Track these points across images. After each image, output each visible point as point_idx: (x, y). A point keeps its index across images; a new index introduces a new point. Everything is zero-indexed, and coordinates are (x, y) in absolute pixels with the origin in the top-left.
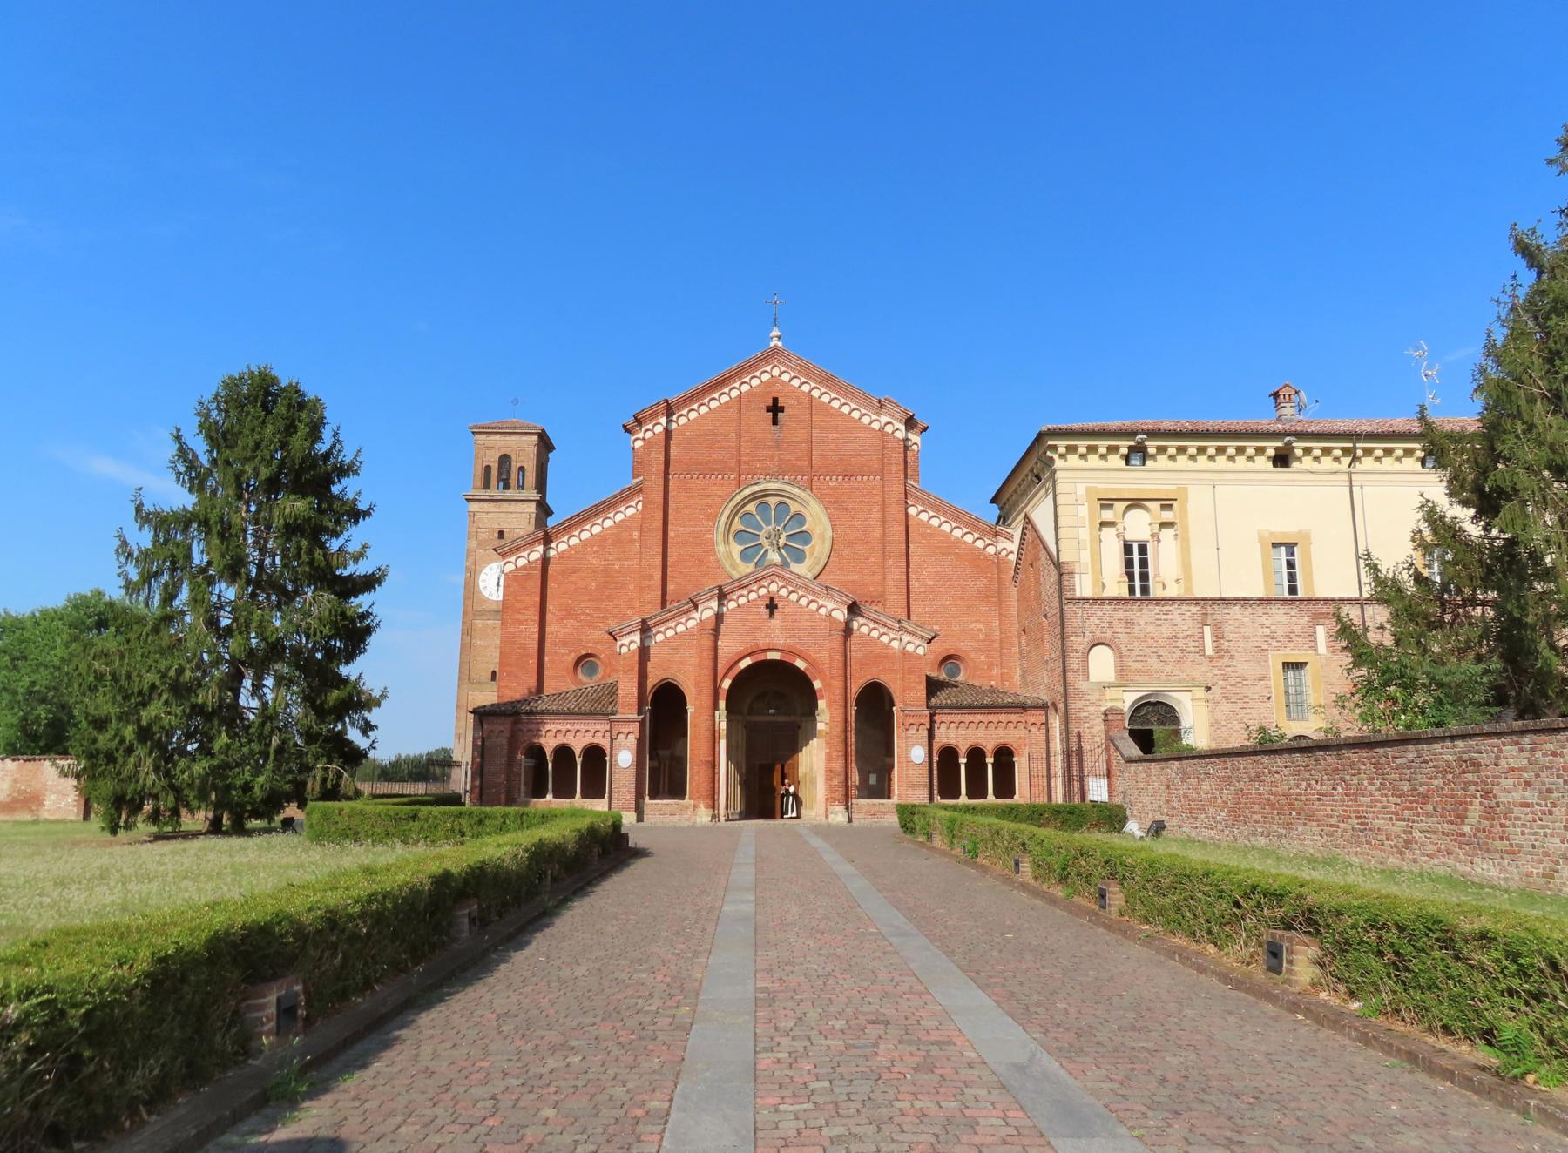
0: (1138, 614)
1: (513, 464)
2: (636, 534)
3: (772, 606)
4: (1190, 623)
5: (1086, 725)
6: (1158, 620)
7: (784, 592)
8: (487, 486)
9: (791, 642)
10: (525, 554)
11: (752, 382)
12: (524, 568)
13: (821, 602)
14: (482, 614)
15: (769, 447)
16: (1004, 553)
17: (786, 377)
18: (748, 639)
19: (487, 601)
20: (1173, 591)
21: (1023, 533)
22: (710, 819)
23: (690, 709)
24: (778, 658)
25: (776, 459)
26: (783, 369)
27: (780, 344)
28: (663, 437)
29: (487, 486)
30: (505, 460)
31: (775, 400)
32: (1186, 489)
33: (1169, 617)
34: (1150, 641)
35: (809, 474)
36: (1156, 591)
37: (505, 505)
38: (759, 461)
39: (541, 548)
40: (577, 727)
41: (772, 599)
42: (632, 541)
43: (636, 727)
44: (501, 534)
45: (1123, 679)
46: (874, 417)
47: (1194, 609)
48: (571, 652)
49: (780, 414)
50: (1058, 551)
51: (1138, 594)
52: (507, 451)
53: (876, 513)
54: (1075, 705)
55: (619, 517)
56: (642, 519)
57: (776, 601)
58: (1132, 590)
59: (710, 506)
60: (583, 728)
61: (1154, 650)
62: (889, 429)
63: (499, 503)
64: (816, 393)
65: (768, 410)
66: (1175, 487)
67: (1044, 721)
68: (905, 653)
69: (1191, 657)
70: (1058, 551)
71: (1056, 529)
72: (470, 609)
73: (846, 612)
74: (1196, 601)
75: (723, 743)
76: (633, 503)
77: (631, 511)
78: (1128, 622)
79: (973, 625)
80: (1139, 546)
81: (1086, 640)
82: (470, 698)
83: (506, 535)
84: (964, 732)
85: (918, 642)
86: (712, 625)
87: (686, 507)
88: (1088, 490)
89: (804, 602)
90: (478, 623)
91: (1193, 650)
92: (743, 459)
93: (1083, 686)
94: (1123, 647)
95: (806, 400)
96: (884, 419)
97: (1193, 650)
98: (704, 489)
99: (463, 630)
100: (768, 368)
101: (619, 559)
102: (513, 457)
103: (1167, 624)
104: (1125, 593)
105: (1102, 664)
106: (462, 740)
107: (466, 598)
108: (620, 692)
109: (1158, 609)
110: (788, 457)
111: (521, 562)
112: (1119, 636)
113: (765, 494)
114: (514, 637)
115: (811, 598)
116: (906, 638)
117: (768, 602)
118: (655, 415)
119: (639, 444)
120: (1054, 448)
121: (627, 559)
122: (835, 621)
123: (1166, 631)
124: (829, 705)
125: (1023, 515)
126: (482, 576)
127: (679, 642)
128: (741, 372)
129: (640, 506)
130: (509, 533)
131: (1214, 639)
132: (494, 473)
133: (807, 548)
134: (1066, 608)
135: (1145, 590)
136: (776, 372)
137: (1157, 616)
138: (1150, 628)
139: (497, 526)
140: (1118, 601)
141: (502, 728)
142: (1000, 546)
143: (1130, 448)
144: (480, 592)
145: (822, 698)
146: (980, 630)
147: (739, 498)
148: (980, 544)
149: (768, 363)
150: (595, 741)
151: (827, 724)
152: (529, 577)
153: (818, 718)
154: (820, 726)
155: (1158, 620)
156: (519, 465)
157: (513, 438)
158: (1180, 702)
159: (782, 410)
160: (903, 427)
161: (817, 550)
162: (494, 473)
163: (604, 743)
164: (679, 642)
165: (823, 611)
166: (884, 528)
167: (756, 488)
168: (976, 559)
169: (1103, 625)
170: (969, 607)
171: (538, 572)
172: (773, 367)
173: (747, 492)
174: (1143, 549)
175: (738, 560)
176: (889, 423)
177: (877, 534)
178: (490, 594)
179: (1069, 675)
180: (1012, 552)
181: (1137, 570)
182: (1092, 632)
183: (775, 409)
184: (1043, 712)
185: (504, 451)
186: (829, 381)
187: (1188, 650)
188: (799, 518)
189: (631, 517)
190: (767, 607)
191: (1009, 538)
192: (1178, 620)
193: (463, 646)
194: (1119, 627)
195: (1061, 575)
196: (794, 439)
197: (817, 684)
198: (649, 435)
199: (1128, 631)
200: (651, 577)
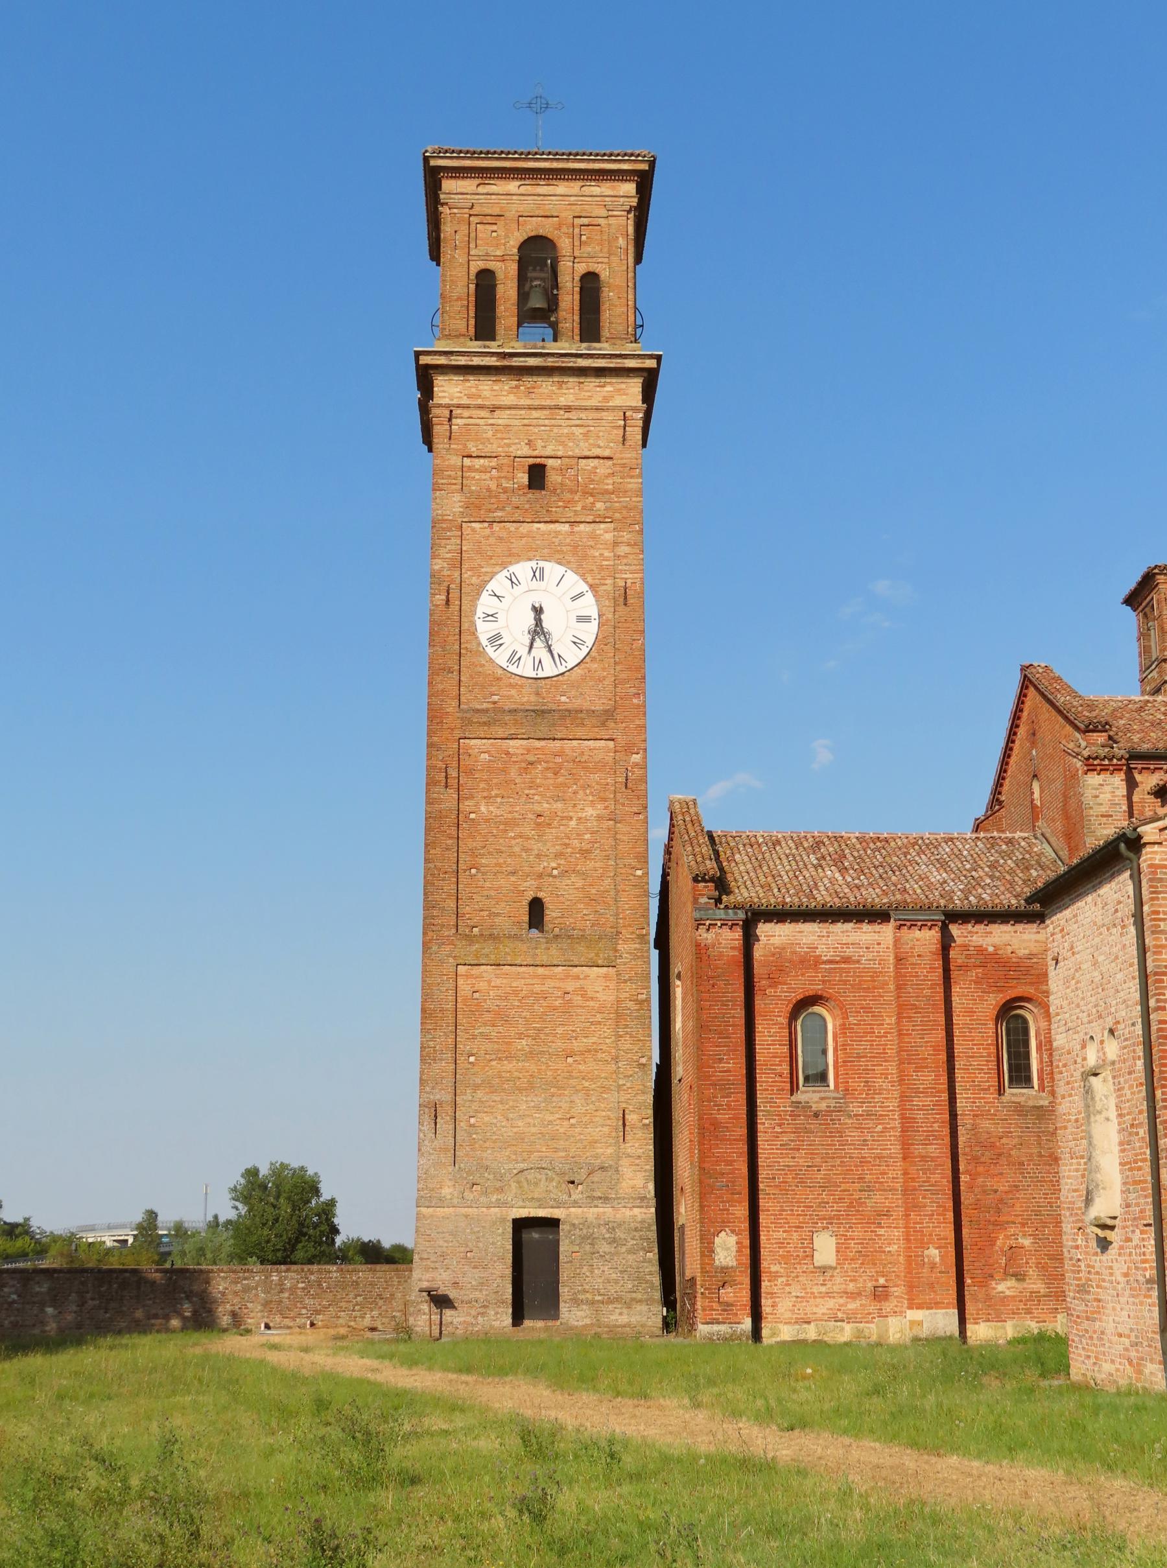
1: (565, 265)
8: (485, 328)
14: (493, 717)
19: (501, 678)
29: (485, 328)
37: (546, 387)
44: (537, 475)
52: (545, 228)
63: (529, 381)
82: (464, 987)
83: (553, 478)
90: (480, 749)
99: (430, 768)
102: (564, 245)
106: (444, 1124)
107: (436, 671)
126: (485, 604)
132: (507, 292)
139: (526, 451)
144: (483, 653)
156: (581, 269)
157: (562, 188)
162: (507, 292)
178: (514, 658)
193: (433, 822)
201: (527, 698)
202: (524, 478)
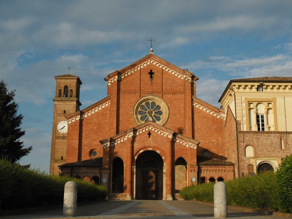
0: (261, 136)
1: (69, 88)
2: (108, 112)
3: (149, 134)
4: (277, 139)
5: (245, 170)
6: (267, 138)
7: (153, 130)
9: (155, 145)
10: (74, 118)
11: (144, 65)
12: (74, 122)
13: (164, 133)
14: (59, 138)
15: (150, 85)
16: (222, 118)
17: (154, 64)
18: (142, 144)
20: (272, 129)
21: (227, 112)
22: (130, 199)
23: (125, 165)
24: (151, 150)
25: (152, 89)
26: (154, 61)
27: (153, 53)
28: (116, 82)
30: (66, 87)
31: (151, 70)
32: (276, 98)
33: (270, 137)
34: (264, 145)
35: (162, 94)
36: (266, 129)
38: (146, 89)
39: (79, 116)
40: (90, 171)
41: (149, 132)
42: (107, 114)
43: (108, 171)
44: (65, 112)
45: (256, 157)
46: (182, 75)
47: (278, 135)
48: (88, 148)
49: (153, 75)
50: (236, 117)
51: (261, 130)
53: (182, 105)
54: (241, 164)
55: (103, 107)
56: (110, 107)
57: (151, 132)
58: (259, 129)
59: (131, 103)
60: (92, 171)
61: (265, 147)
62: (186, 79)
64: (164, 68)
65: (149, 73)
66: (272, 98)
67: (233, 169)
68: (190, 148)
69: (277, 150)
70: (236, 117)
71: (236, 110)
72: (54, 136)
73: (172, 136)
74: (279, 132)
75: (135, 176)
76: (108, 103)
77: (107, 105)
78: (258, 139)
79: (213, 140)
80: (261, 115)
81: (245, 144)
82: (54, 165)
83: (66, 112)
84: (208, 173)
85: (194, 145)
86: (131, 140)
87: (124, 104)
88: (245, 98)
89: (159, 133)
90: (57, 141)
91: (278, 147)
92: (142, 89)
93: (244, 158)
94: (256, 146)
95: (161, 71)
96: (185, 76)
97: (278, 147)
98: (129, 98)
100: (149, 61)
101: (103, 120)
102: (69, 86)
103: (270, 139)
104: (257, 130)
105: (250, 152)
108: (103, 160)
109: (267, 135)
110: (155, 88)
111: (73, 121)
112: (255, 143)
113: (148, 99)
114: (71, 144)
115: (161, 131)
116: (190, 144)
117: (148, 133)
118: (113, 76)
119: (109, 84)
120: (235, 86)
121: (105, 120)
122: (169, 138)
123: (269, 142)
124: (167, 164)
125: (227, 106)
127: (121, 145)
128: (141, 62)
129: (110, 103)
130: (67, 111)
131: (284, 144)
132: (63, 92)
133: (161, 116)
134: (238, 134)
135: (263, 129)
136: (151, 62)
137: (267, 137)
138: (264, 141)
139: (63, 109)
140: (254, 132)
141: (68, 171)
142: (221, 115)
143: (258, 86)
145: (165, 162)
146: (215, 142)
147: (140, 101)
148: (215, 115)
149: (149, 59)
150: (96, 175)
151: (166, 170)
152: (76, 125)
153: (164, 168)
154: (164, 171)
155: (267, 138)
156: (70, 89)
157: (69, 80)
158: (274, 163)
159: (153, 73)
160: (191, 79)
161: (164, 117)
163: (99, 176)
164: (121, 145)
165: (165, 135)
166: (185, 110)
167: (145, 98)
168: (214, 119)
169: (250, 140)
170: (211, 134)
171: (78, 124)
172: (151, 60)
173: (143, 99)
174: (262, 117)
175: (140, 120)
176: (186, 77)
177: (183, 112)
179: (239, 155)
180: (225, 117)
181: (260, 123)
182: (246, 142)
183: (151, 73)
184: (233, 167)
185: (66, 84)
186: (168, 64)
187: (276, 147)
188: (159, 107)
189: (107, 106)
190: (148, 134)
191: (224, 113)
192: (273, 138)
194: (255, 141)
195: (237, 124)
196: (157, 82)
197: (163, 158)
198: (112, 81)
199: (258, 141)
200: (113, 125)
201: (62, 135)
202: (63, 112)
